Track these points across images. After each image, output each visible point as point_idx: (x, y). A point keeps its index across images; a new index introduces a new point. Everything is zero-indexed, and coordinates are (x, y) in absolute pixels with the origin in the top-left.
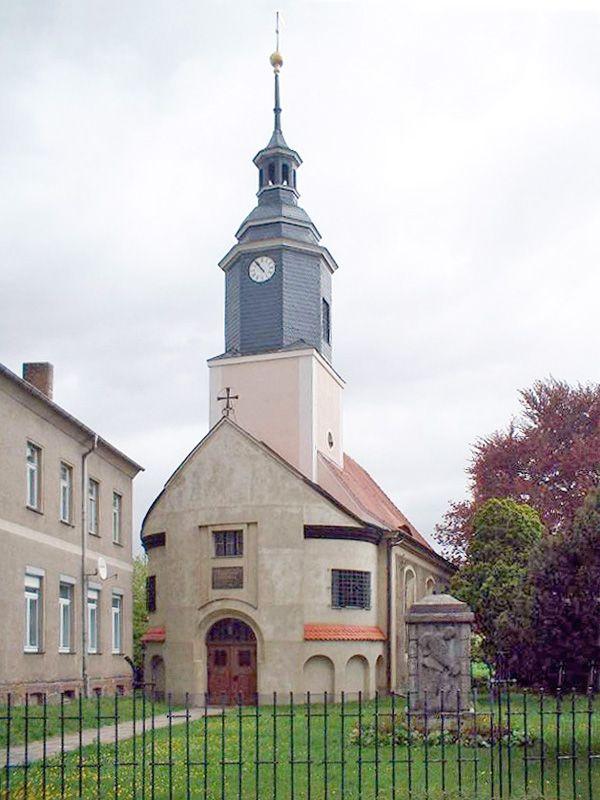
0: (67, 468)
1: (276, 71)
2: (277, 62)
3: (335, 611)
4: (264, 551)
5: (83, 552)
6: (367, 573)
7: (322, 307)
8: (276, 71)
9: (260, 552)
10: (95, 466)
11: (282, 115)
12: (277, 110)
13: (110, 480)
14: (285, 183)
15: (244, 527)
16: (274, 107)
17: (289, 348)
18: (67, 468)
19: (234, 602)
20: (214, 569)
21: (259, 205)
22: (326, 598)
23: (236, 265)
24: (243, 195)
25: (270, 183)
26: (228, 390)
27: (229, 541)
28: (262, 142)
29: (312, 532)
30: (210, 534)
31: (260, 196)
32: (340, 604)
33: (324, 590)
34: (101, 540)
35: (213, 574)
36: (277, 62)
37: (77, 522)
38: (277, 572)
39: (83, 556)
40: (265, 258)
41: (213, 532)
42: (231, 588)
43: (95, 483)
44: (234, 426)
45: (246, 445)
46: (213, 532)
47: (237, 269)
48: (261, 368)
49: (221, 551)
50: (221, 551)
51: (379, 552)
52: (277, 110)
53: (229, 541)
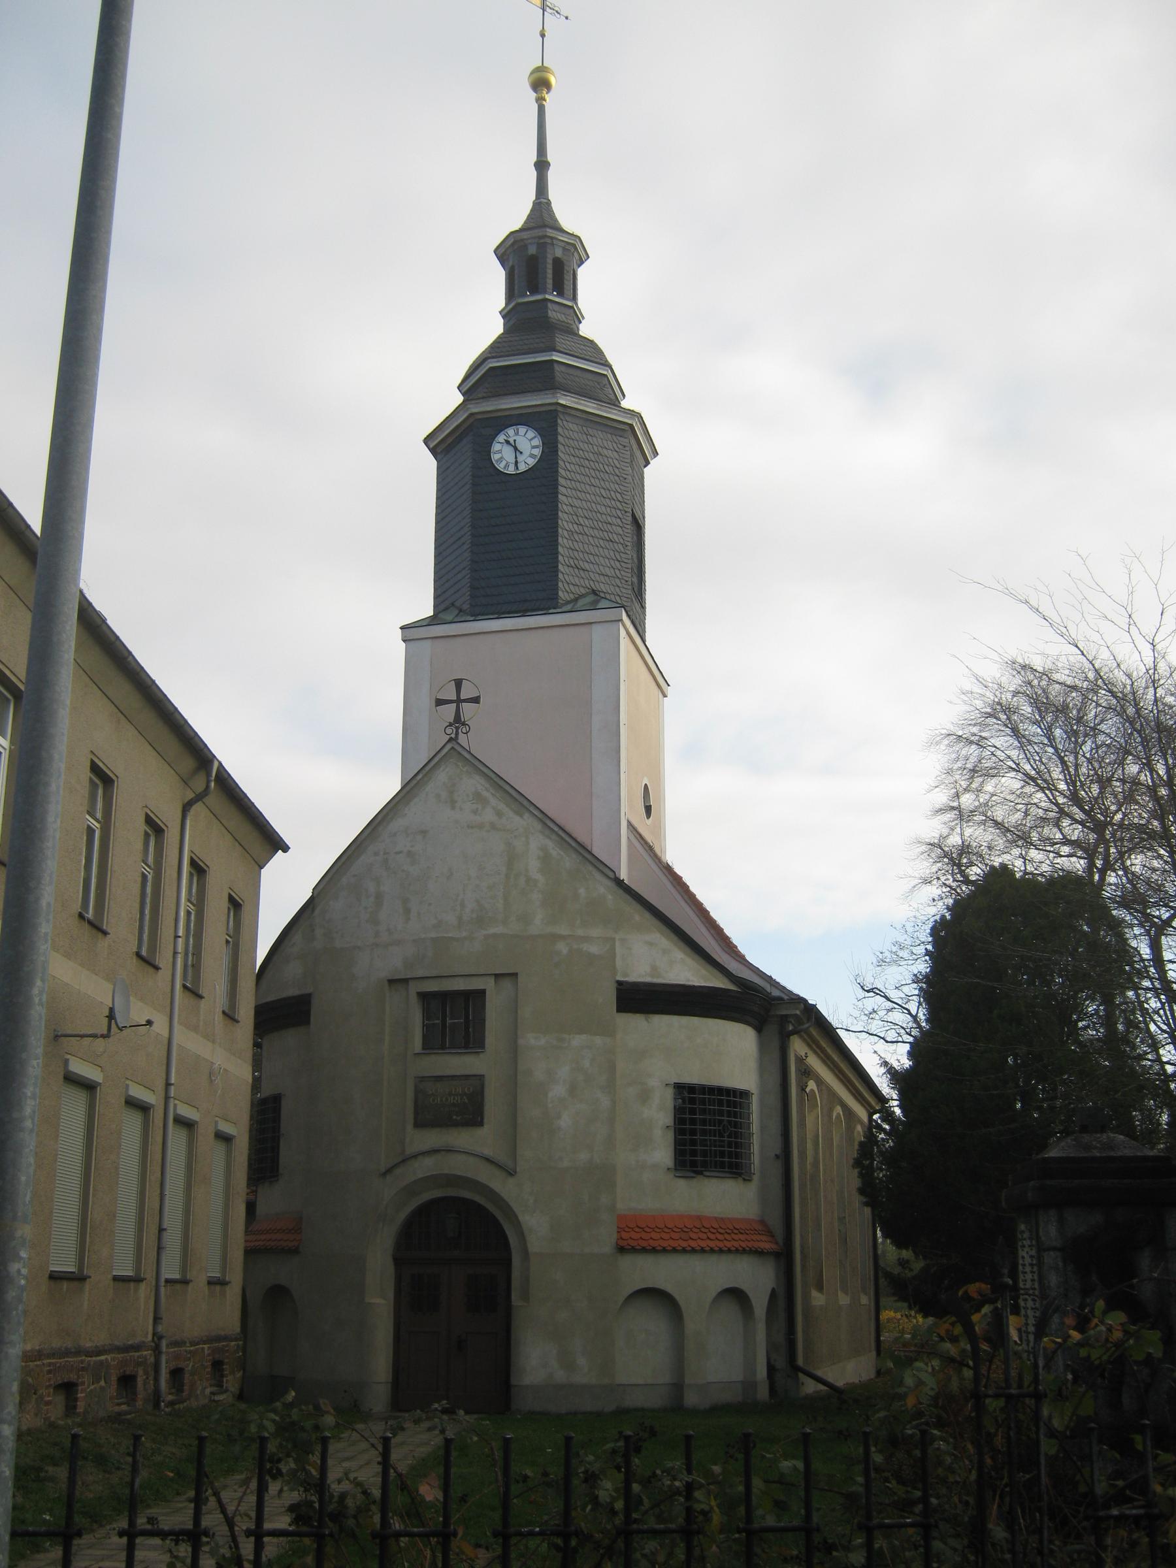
0: (155, 828)
1: (540, 101)
2: (540, 83)
3: (682, 1183)
4: (532, 1040)
6: (745, 1094)
8: (540, 101)
9: (521, 1042)
10: (203, 835)
11: (552, 175)
12: (542, 166)
15: (488, 985)
16: (534, 158)
17: (573, 606)
19: (467, 1153)
20: (422, 1079)
21: (508, 330)
22: (662, 1153)
27: (454, 1015)
28: (515, 216)
29: (640, 999)
30: (414, 999)
31: (506, 315)
32: (693, 1164)
33: (658, 1133)
35: (417, 1091)
36: (540, 83)
37: (164, 960)
38: (558, 1091)
40: (522, 430)
41: (419, 994)
42: (456, 1124)
44: (477, 766)
45: (493, 801)
46: (419, 994)
48: (508, 647)
49: (435, 1041)
50: (435, 1041)
51: (762, 1047)
52: (542, 166)
53: (454, 1015)
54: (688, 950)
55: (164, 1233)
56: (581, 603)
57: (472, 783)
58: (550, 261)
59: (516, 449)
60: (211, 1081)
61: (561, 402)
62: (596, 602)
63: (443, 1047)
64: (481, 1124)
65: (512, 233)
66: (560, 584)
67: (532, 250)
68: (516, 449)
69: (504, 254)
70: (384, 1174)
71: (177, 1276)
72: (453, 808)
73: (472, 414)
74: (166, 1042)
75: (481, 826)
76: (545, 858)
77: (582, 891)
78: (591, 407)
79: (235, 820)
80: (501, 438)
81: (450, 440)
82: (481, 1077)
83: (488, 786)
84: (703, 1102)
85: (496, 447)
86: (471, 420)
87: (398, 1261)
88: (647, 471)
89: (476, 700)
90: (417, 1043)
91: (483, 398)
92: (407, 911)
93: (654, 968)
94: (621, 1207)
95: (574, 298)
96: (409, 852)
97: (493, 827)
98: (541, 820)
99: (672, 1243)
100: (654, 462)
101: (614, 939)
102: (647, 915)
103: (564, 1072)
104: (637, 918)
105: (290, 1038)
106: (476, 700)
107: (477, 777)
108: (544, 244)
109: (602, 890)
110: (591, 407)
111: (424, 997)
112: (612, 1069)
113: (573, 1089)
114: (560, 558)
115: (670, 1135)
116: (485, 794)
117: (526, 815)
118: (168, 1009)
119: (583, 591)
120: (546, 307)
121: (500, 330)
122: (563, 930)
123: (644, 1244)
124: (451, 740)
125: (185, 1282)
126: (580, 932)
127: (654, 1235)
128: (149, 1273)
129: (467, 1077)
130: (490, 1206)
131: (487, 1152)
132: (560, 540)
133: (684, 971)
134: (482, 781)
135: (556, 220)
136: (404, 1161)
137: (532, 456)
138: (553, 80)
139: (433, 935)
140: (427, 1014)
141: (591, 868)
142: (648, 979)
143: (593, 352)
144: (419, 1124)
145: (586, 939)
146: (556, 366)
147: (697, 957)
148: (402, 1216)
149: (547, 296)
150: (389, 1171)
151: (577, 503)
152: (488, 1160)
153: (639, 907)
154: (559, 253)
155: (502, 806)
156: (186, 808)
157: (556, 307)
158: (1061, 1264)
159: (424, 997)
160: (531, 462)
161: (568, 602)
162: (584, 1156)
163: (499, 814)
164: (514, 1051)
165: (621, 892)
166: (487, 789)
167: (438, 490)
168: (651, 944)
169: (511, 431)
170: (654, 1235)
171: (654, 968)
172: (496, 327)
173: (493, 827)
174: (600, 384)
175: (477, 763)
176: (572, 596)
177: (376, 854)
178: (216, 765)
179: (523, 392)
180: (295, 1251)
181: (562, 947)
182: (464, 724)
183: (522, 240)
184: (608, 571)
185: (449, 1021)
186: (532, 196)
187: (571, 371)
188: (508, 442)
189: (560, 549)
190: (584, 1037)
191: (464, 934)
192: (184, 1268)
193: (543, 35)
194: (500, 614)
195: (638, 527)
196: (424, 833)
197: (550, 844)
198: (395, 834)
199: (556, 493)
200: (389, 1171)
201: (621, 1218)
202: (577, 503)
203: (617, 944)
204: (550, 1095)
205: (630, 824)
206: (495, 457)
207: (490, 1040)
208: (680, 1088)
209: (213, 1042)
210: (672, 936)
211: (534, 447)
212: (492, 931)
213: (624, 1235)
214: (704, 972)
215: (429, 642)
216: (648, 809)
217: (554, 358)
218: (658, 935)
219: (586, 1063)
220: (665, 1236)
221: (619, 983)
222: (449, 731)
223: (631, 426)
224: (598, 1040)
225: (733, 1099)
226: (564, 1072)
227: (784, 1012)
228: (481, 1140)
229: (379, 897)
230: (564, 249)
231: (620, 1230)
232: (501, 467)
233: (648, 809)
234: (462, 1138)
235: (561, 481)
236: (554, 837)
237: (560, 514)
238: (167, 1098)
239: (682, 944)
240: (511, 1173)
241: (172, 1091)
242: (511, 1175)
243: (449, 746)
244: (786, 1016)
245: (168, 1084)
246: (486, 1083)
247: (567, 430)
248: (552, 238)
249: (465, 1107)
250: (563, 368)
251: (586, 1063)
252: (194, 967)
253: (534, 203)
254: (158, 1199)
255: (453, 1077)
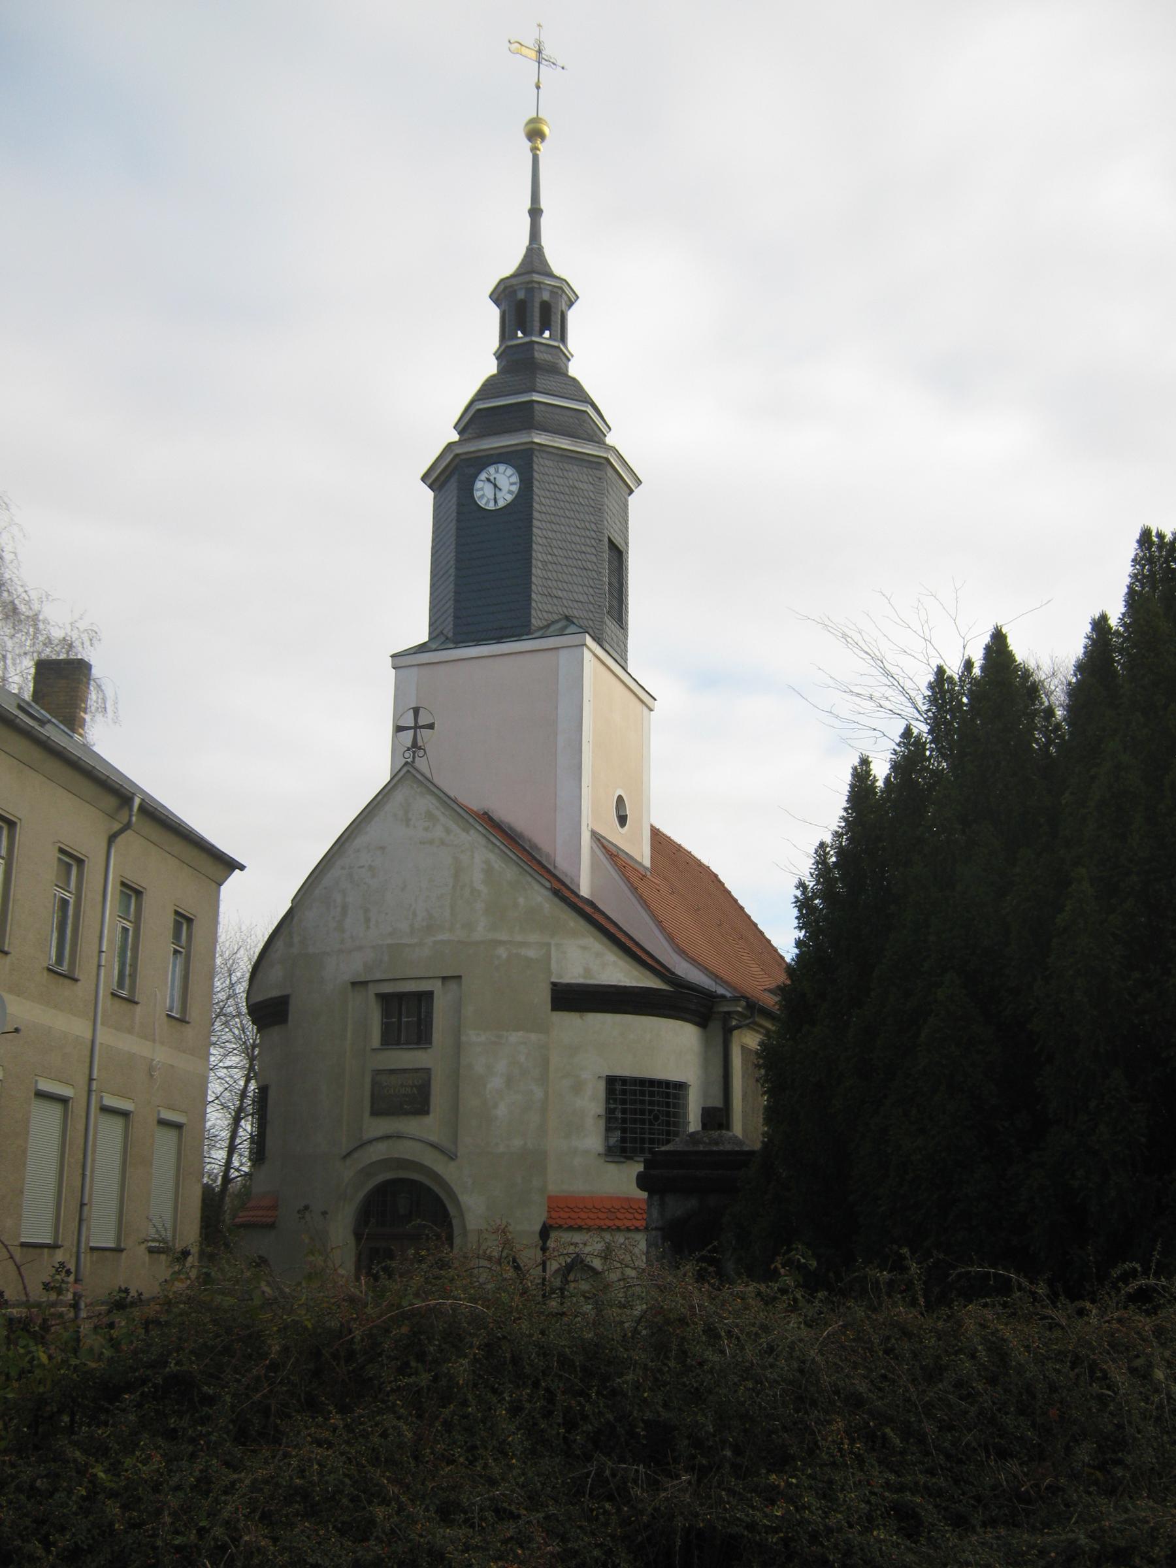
0: (71, 861)
1: (534, 150)
2: (535, 134)
3: (612, 1168)
4: (474, 1037)
5: (94, 1030)
6: (681, 1086)
7: (606, 556)
8: (534, 150)
9: (463, 1038)
10: (137, 858)
11: (544, 221)
12: (535, 213)
13: (166, 885)
14: (547, 334)
15: (436, 986)
16: (528, 205)
17: (545, 632)
18: (71, 861)
19: (414, 1139)
20: (378, 1072)
21: (502, 370)
23: (451, 476)
24: (470, 355)
25: (520, 334)
26: (416, 711)
27: (407, 1014)
28: (509, 262)
29: (573, 998)
31: (499, 356)
32: (623, 1150)
33: (590, 1122)
34: (138, 1008)
35: (374, 1083)
36: (535, 134)
37: (86, 972)
39: (93, 1042)
40: (502, 467)
41: (378, 995)
42: (406, 1113)
43: (132, 892)
44: (428, 786)
45: (443, 819)
46: (378, 995)
47: (453, 485)
49: (391, 1037)
50: (391, 1037)
51: (707, 1042)
52: (535, 213)
53: (407, 1014)
54: (621, 953)
55: (86, 1208)
56: (552, 629)
57: (425, 803)
58: (537, 305)
59: (495, 486)
60: (152, 1076)
61: (537, 440)
62: (566, 627)
63: (398, 1043)
64: (427, 1113)
65: (502, 280)
66: (533, 612)
67: (521, 295)
68: (495, 486)
69: (495, 296)
70: (345, 1157)
71: (112, 1245)
72: (408, 826)
73: (457, 455)
74: (89, 1044)
75: (431, 842)
76: (489, 871)
77: (521, 900)
78: (565, 443)
79: (178, 846)
80: (483, 476)
81: (442, 478)
82: (428, 1071)
83: (438, 804)
84: (634, 1093)
85: (478, 484)
86: (457, 460)
87: (358, 1236)
88: (632, 500)
89: (431, 726)
90: (376, 1039)
91: (474, 438)
92: (368, 920)
93: (587, 970)
94: (553, 1189)
95: (563, 339)
96: (370, 866)
97: (443, 843)
98: (484, 836)
99: (598, 1222)
100: (637, 491)
101: (549, 945)
102: (582, 922)
103: (501, 1066)
104: (572, 924)
105: (275, 1033)
106: (431, 726)
107: (429, 797)
108: (531, 288)
109: (540, 899)
110: (565, 443)
111: (383, 998)
112: (545, 1062)
113: (509, 1081)
114: (533, 587)
115: (602, 1123)
116: (437, 813)
117: (472, 832)
118: (92, 1014)
119: (556, 617)
120: (533, 349)
121: (494, 370)
122: (503, 937)
123: (572, 1223)
124: (407, 763)
125: (118, 1250)
126: (519, 938)
127: (583, 1215)
128: (68, 1241)
129: (417, 1070)
130: (436, 1188)
131: (433, 1138)
132: (534, 570)
133: (617, 972)
134: (434, 801)
135: (546, 264)
136: (361, 1146)
137: (510, 492)
138: (546, 130)
139: (389, 941)
140: (386, 1013)
141: (530, 879)
142: (581, 981)
143: (577, 391)
144: (376, 1113)
145: (524, 944)
146: (536, 406)
147: (629, 959)
148: (361, 1195)
149: (534, 339)
150: (349, 1154)
151: (550, 534)
152: (433, 1146)
153: (574, 915)
154: (546, 296)
155: (452, 825)
156: (112, 839)
157: (543, 348)
158: (660, 1241)
159: (383, 998)
160: (510, 498)
161: (541, 628)
162: (517, 1143)
163: (448, 831)
164: (458, 1047)
165: (556, 900)
166: (437, 808)
167: (434, 525)
168: (584, 948)
169: (492, 469)
170: (583, 1215)
171: (587, 970)
172: (491, 367)
173: (443, 843)
174: (583, 422)
175: (429, 784)
176: (545, 623)
177: (343, 868)
178: (137, 802)
179: (516, 431)
180: (272, 1226)
181: (502, 952)
182: (420, 748)
183: (511, 286)
184: (582, 598)
185: (404, 1020)
186: (525, 242)
187: (550, 409)
188: (488, 480)
189: (534, 579)
190: (520, 1033)
191: (416, 940)
192: (119, 1239)
193: (538, 87)
194: (478, 641)
195: (618, 555)
196: (383, 848)
197: (491, 856)
198: (358, 851)
199: (529, 526)
200: (349, 1154)
201: (550, 1198)
202: (550, 534)
203: (553, 949)
204: (489, 1086)
205: (595, 836)
206: (477, 494)
207: (437, 1036)
208: (611, 1081)
209: (154, 1041)
210: (605, 940)
211: (512, 484)
212: (440, 937)
213: (554, 1215)
214: (635, 973)
215: (415, 669)
216: (623, 820)
217: (535, 398)
218: (592, 940)
219: (522, 1058)
220: (592, 1216)
221: (554, 984)
222: (407, 755)
223: (607, 460)
224: (533, 1037)
225: (673, 1091)
226: (501, 1066)
227: (726, 1009)
228: (429, 1127)
229: (345, 908)
230: (552, 292)
231: (550, 1209)
232: (482, 503)
233: (623, 820)
234: (410, 1125)
235: (536, 514)
236: (497, 851)
237: (534, 546)
238: (90, 1091)
239: (615, 949)
240: (452, 1157)
241: (95, 1085)
242: (452, 1159)
243: (405, 770)
244: (729, 1013)
245: (91, 1079)
246: (433, 1077)
247: (541, 466)
248: (539, 283)
249: (411, 1097)
250: (543, 408)
251: (522, 1058)
252: (128, 975)
253: (528, 249)
254: (79, 1179)
255: (405, 1070)
